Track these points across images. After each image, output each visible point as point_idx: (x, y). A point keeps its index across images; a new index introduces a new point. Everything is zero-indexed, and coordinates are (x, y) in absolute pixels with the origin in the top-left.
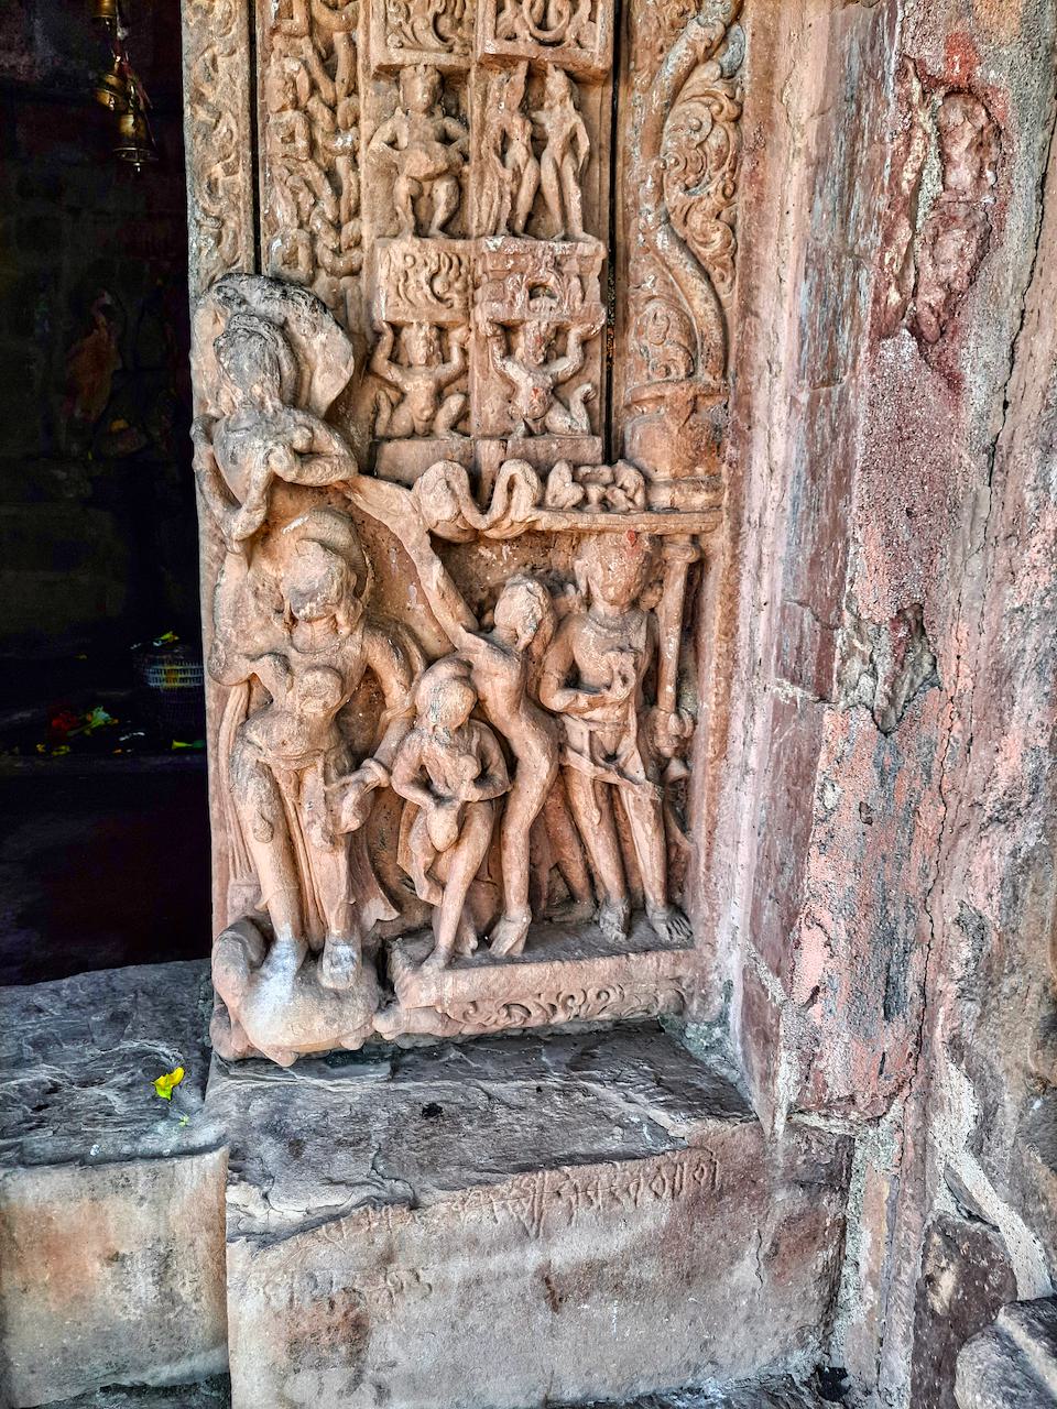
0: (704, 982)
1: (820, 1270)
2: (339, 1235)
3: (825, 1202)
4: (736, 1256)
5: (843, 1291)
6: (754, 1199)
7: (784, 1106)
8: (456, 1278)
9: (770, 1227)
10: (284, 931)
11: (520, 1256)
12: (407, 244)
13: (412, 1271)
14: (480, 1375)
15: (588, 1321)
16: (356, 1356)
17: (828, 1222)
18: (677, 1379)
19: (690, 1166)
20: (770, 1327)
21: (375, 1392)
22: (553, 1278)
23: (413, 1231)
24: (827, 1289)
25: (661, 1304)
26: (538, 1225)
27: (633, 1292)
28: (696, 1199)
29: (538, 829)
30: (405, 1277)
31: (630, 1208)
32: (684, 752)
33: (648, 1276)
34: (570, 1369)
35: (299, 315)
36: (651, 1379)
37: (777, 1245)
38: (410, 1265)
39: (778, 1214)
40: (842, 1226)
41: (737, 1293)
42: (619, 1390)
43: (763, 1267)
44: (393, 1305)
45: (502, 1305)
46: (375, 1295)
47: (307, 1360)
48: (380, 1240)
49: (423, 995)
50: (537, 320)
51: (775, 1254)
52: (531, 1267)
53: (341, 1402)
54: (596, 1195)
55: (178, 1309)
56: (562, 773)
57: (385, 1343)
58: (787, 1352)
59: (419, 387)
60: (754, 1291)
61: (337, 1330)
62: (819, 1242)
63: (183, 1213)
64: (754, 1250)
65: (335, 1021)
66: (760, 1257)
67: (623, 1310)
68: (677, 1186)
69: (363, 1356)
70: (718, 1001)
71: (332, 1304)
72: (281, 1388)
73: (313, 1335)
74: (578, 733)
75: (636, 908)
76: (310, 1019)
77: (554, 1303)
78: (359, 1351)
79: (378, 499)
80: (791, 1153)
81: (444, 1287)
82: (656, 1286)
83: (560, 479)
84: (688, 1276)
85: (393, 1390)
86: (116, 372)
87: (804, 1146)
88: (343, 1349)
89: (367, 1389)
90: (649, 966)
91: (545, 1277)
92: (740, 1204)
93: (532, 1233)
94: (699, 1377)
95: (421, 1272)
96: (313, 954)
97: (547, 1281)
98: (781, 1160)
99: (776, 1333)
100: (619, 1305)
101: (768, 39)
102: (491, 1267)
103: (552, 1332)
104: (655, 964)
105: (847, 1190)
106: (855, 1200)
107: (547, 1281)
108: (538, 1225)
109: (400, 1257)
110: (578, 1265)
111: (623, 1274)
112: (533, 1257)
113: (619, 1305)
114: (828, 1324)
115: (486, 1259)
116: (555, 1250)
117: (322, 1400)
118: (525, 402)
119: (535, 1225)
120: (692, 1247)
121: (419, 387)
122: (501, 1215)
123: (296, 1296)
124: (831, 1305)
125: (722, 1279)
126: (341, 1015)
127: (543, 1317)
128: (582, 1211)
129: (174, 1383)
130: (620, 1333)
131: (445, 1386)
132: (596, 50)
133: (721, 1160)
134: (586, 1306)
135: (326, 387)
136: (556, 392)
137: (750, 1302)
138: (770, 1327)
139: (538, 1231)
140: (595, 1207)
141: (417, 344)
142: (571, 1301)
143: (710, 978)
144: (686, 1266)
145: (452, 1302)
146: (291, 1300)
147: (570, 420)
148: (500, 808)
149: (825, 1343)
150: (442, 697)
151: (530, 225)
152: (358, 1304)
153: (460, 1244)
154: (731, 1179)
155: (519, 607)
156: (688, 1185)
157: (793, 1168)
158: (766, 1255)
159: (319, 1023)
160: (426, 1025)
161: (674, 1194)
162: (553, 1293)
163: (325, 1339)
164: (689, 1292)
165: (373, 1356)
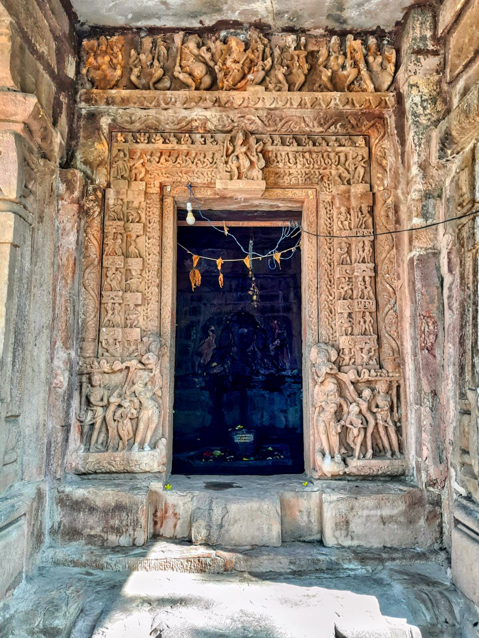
0: (408, 467)
4: (420, 518)
9: (426, 513)
10: (327, 452)
12: (345, 337)
15: (390, 529)
16: (347, 529)
23: (356, 504)
28: (410, 505)
29: (372, 434)
30: (355, 513)
32: (400, 420)
33: (402, 520)
35: (329, 348)
39: (427, 510)
40: (441, 514)
48: (351, 505)
50: (367, 347)
56: (377, 424)
57: (353, 526)
58: (433, 543)
59: (347, 358)
70: (412, 471)
74: (379, 416)
75: (393, 454)
79: (342, 376)
80: (428, 497)
81: (362, 516)
83: (372, 372)
86: (214, 349)
89: (349, 537)
90: (397, 463)
96: (333, 457)
98: (426, 498)
101: (401, 306)
112: (379, 513)
118: (365, 360)
121: (347, 358)
127: (382, 526)
132: (373, 308)
135: (333, 359)
136: (370, 358)
141: (346, 351)
147: (373, 362)
148: (365, 429)
149: (442, 542)
150: (354, 409)
151: (364, 334)
155: (367, 393)
157: (429, 500)
159: (335, 467)
160: (354, 471)
161: (405, 503)
163: (342, 524)
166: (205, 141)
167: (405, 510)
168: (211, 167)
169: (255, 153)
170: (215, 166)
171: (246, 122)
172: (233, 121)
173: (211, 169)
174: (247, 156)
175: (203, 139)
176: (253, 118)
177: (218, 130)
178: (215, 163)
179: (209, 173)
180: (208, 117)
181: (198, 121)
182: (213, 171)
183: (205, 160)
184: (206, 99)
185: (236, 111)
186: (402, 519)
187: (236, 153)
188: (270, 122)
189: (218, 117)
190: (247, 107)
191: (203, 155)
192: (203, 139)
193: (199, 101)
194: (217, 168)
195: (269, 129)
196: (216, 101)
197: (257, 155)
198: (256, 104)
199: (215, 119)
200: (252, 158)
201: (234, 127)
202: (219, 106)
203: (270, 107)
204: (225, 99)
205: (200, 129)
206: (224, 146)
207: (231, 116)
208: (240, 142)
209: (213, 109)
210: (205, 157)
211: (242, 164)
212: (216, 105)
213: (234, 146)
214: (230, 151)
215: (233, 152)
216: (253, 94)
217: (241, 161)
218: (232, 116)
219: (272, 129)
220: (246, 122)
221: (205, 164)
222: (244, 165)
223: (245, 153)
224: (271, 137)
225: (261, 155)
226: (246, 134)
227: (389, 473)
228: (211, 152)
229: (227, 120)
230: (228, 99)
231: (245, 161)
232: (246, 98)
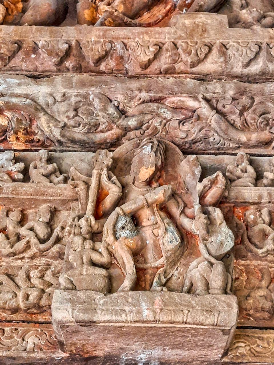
166: (25, 172)
168: (42, 253)
169: (197, 207)
170: (55, 249)
171: (168, 115)
172: (123, 113)
173: (44, 261)
174: (170, 216)
175: (21, 165)
176: (191, 103)
177: (73, 141)
178: (58, 240)
179: (34, 274)
180: (41, 101)
181: (8, 114)
182: (48, 266)
183: (23, 231)
184: (35, 49)
185: (134, 84)
187: (128, 207)
188: (249, 116)
189: (73, 100)
190: (168, 72)
191: (15, 215)
192: (21, 165)
193: (14, 54)
194: (60, 256)
195: (243, 138)
196: (68, 53)
197: (205, 212)
198: (200, 61)
199: (62, 107)
200: (185, 222)
201: (126, 130)
202: (79, 69)
203: (246, 71)
204: (99, 47)
205: (11, 138)
206: (87, 184)
207: (119, 97)
208: (146, 173)
209: (59, 79)
210: (22, 222)
211: (149, 242)
212: (69, 64)
213: (124, 187)
214: (108, 202)
215: (120, 201)
216: (191, 35)
217: (147, 233)
218: (120, 97)
219: (254, 137)
220: (168, 115)
221: (20, 245)
222: (157, 247)
223: (163, 208)
224: (251, 163)
225: (217, 214)
226: (166, 150)
228: (44, 207)
229: (104, 109)
230: (108, 46)
231: (161, 232)
232: (168, 45)
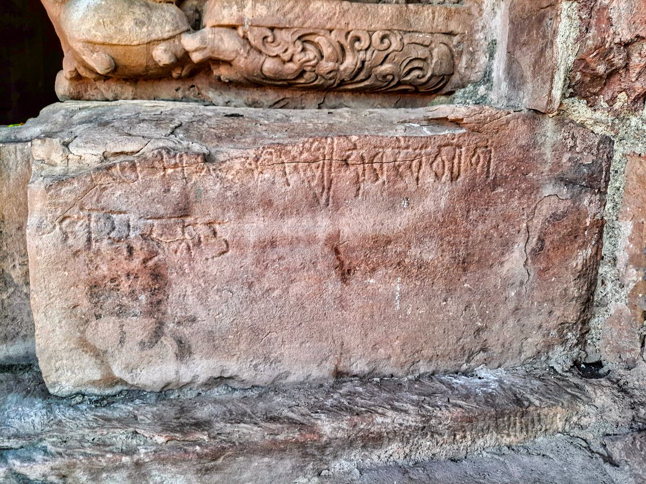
0: (471, 41)
1: (579, 267)
2: (133, 176)
3: (586, 202)
4: (506, 245)
5: (600, 289)
6: (524, 193)
7: (562, 68)
8: (252, 238)
9: (537, 222)
11: (311, 223)
13: (209, 224)
14: (276, 338)
15: (373, 296)
16: (156, 307)
17: (588, 221)
18: (453, 363)
19: (468, 150)
20: (535, 320)
21: (176, 346)
22: (341, 250)
24: (585, 288)
25: (440, 285)
26: (328, 192)
27: (414, 271)
28: (470, 189)
30: (203, 231)
31: (412, 187)
33: (428, 257)
34: (358, 341)
36: (431, 361)
37: (543, 241)
38: (207, 219)
39: (545, 210)
40: (600, 225)
41: (507, 284)
42: (402, 366)
43: (530, 261)
44: (191, 259)
45: (295, 270)
46: (174, 246)
47: (109, 304)
48: (176, 189)
49: (225, 12)
51: (541, 249)
52: (321, 235)
53: (144, 354)
54: (381, 168)
55: (11, 290)
58: (549, 346)
60: (522, 283)
61: (136, 277)
62: (580, 241)
63: (9, 196)
64: (522, 245)
65: (143, 23)
66: (528, 251)
67: (405, 287)
68: (455, 169)
69: (163, 308)
70: (483, 60)
71: (130, 250)
72: (83, 332)
73: (113, 280)
76: (120, 18)
77: (343, 274)
78: (159, 302)
80: (559, 149)
81: (241, 246)
82: (436, 267)
84: (464, 263)
85: (193, 347)
87: (570, 143)
88: (143, 298)
89: (168, 345)
91: (335, 245)
92: (512, 195)
93: (323, 201)
94: (472, 364)
95: (217, 227)
97: (337, 251)
98: (549, 154)
99: (540, 327)
100: (402, 282)
102: (285, 230)
103: (342, 303)
104: (431, 16)
105: (606, 193)
106: (613, 200)
107: (337, 251)
108: (328, 192)
109: (197, 208)
110: (364, 238)
111: (405, 253)
112: (323, 225)
113: (402, 282)
114: (584, 322)
115: (280, 222)
116: (343, 221)
117: (124, 350)
119: (325, 194)
120: (468, 234)
122: (293, 179)
123: (93, 236)
124: (588, 303)
125: (494, 269)
126: (149, 19)
127: (333, 286)
128: (366, 186)
129: (11, 362)
130: (403, 311)
131: (243, 346)
133: (495, 148)
134: (372, 281)
137: (518, 294)
138: (535, 320)
139: (328, 200)
140: (380, 181)
142: (358, 274)
143: (477, 37)
144: (462, 253)
145: (248, 261)
146: (89, 240)
149: (582, 342)
152: (157, 254)
153: (255, 204)
154: (504, 169)
156: (466, 171)
157: (558, 164)
158: (533, 250)
159: (128, 24)
161: (453, 178)
162: (342, 264)
163: (125, 286)
164: (464, 278)
165: (172, 309)
167: (450, 211)
186: (429, 253)
227: (387, 67)
